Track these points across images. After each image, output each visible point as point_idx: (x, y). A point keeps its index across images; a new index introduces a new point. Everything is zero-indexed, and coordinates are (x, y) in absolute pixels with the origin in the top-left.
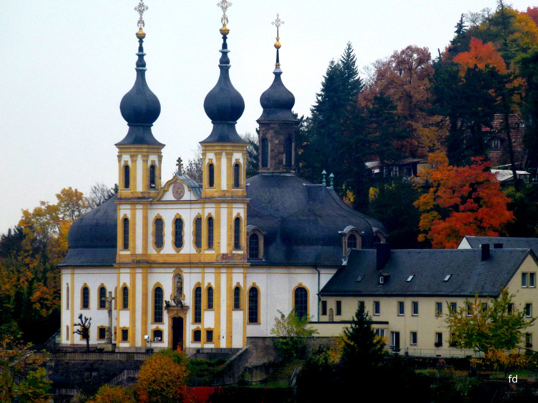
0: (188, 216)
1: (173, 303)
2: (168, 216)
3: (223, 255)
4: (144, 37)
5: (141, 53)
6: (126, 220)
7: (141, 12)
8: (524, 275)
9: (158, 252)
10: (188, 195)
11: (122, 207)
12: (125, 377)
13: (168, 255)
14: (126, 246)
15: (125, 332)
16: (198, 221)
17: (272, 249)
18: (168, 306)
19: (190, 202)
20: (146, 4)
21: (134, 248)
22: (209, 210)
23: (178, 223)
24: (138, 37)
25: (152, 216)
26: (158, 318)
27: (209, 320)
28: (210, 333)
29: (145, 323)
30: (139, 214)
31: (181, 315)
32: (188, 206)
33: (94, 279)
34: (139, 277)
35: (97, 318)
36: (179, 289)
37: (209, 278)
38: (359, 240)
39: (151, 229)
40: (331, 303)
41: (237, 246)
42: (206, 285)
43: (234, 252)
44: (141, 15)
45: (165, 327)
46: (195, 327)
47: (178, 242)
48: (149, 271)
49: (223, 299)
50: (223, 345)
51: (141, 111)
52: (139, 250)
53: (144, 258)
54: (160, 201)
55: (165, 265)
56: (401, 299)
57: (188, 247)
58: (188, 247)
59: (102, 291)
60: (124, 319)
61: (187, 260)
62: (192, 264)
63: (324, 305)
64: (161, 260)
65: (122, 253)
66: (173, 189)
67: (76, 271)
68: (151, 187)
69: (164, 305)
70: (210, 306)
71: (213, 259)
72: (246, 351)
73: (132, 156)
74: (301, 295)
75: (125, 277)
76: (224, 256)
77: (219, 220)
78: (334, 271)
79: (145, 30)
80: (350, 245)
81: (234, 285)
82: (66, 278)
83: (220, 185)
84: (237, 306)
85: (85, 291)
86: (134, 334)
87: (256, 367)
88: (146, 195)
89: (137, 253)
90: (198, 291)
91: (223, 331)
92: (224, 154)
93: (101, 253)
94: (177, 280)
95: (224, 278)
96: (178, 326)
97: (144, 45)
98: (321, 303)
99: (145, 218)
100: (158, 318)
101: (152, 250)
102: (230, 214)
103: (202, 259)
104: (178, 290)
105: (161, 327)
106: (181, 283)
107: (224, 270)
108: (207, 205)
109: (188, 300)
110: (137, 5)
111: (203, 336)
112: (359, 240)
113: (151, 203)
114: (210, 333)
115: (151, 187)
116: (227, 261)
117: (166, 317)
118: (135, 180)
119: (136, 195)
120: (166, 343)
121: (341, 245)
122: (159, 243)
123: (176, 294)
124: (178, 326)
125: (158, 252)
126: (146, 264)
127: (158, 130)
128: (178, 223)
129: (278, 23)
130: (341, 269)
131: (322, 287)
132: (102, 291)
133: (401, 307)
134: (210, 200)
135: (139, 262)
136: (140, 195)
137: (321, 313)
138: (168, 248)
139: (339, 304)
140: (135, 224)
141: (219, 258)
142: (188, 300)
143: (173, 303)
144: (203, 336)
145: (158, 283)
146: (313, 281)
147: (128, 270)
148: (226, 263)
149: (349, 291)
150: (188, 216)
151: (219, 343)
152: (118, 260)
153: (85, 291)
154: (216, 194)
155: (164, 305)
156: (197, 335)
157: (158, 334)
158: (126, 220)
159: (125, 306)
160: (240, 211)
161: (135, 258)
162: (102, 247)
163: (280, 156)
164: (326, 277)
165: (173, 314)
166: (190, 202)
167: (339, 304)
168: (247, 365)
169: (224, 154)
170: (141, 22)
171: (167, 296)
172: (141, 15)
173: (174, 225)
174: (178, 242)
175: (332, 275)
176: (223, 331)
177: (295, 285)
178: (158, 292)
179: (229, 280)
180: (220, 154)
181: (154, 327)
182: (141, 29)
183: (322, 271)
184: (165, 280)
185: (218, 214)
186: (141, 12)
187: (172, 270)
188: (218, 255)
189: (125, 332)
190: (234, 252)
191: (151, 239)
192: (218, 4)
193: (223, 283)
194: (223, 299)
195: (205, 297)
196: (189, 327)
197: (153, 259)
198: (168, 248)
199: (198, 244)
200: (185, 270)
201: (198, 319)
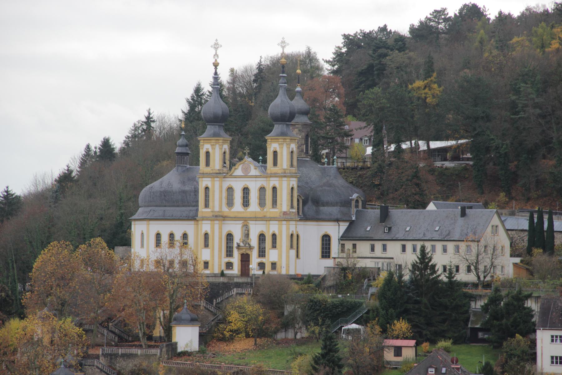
0: (254, 187)
2: (238, 186)
3: (284, 212)
4: (218, 66)
5: (216, 76)
6: (207, 188)
7: (216, 49)
8: (493, 226)
9: (230, 210)
10: (254, 172)
12: (234, 293)
13: (238, 212)
14: (207, 206)
15: (206, 264)
16: (262, 190)
17: (306, 208)
18: (238, 246)
19: (256, 177)
20: (220, 43)
21: (213, 207)
22: (274, 182)
23: (246, 191)
24: (214, 65)
26: (229, 253)
27: (272, 255)
28: (274, 265)
29: (220, 258)
31: (248, 252)
32: (254, 179)
34: (217, 227)
36: (247, 235)
37: (274, 227)
38: (360, 204)
39: (224, 194)
40: (349, 245)
41: (292, 207)
42: (271, 232)
43: (291, 210)
44: (216, 51)
45: (236, 260)
46: (260, 260)
47: (246, 203)
49: (283, 241)
50: (284, 272)
52: (217, 209)
53: (220, 214)
54: (232, 176)
56: (404, 243)
57: (254, 206)
58: (254, 206)
59: (172, 235)
62: (256, 219)
63: (343, 245)
64: (232, 215)
67: (151, 222)
68: (224, 166)
70: (274, 246)
71: (277, 215)
72: (325, 276)
73: (212, 145)
74: (326, 239)
76: (285, 213)
77: (281, 189)
78: (347, 224)
79: (218, 61)
80: (357, 206)
81: (291, 233)
83: (282, 165)
84: (292, 247)
85: (158, 236)
86: (213, 265)
87: (330, 287)
88: (221, 172)
89: (215, 210)
90: (262, 237)
91: (284, 264)
92: (285, 144)
93: (185, 211)
94: (244, 228)
95: (284, 227)
96: (245, 259)
97: (218, 70)
98: (340, 245)
99: (221, 187)
100: (229, 253)
101: (225, 209)
102: (289, 185)
103: (268, 215)
104: (245, 236)
106: (248, 231)
107: (284, 222)
110: (213, 44)
112: (360, 204)
113: (225, 177)
114: (274, 265)
115: (224, 166)
116: (287, 216)
118: (214, 161)
119: (214, 171)
120: (236, 270)
121: (351, 206)
122: (230, 203)
123: (244, 238)
124: (245, 259)
125: (230, 210)
126: (221, 218)
128: (246, 191)
130: (352, 223)
131: (341, 234)
132: (172, 235)
133: (404, 248)
134: (275, 175)
135: (216, 216)
136: (218, 172)
137: (340, 251)
139: (354, 246)
140: (214, 191)
141: (282, 214)
142: (254, 241)
143: (242, 244)
146: (335, 231)
148: (285, 217)
149: (353, 237)
150: (254, 187)
151: (281, 271)
152: (200, 215)
153: (158, 236)
154: (280, 172)
155: (235, 245)
156: (262, 266)
157: (229, 265)
158: (207, 188)
159: (206, 245)
161: (214, 214)
162: (169, 206)
164: (344, 226)
166: (256, 177)
167: (354, 246)
168: (325, 285)
169: (285, 144)
170: (216, 55)
171: (237, 239)
172: (216, 51)
173: (242, 192)
174: (246, 203)
175: (346, 227)
176: (284, 264)
177: (323, 233)
178: (230, 237)
179: (288, 229)
180: (282, 144)
182: (216, 60)
183: (341, 223)
185: (281, 185)
186: (216, 49)
188: (281, 212)
189: (206, 264)
190: (291, 210)
191: (224, 201)
192: (278, 44)
193: (283, 231)
194: (283, 241)
196: (255, 260)
197: (225, 214)
199: (262, 203)
200: (250, 222)
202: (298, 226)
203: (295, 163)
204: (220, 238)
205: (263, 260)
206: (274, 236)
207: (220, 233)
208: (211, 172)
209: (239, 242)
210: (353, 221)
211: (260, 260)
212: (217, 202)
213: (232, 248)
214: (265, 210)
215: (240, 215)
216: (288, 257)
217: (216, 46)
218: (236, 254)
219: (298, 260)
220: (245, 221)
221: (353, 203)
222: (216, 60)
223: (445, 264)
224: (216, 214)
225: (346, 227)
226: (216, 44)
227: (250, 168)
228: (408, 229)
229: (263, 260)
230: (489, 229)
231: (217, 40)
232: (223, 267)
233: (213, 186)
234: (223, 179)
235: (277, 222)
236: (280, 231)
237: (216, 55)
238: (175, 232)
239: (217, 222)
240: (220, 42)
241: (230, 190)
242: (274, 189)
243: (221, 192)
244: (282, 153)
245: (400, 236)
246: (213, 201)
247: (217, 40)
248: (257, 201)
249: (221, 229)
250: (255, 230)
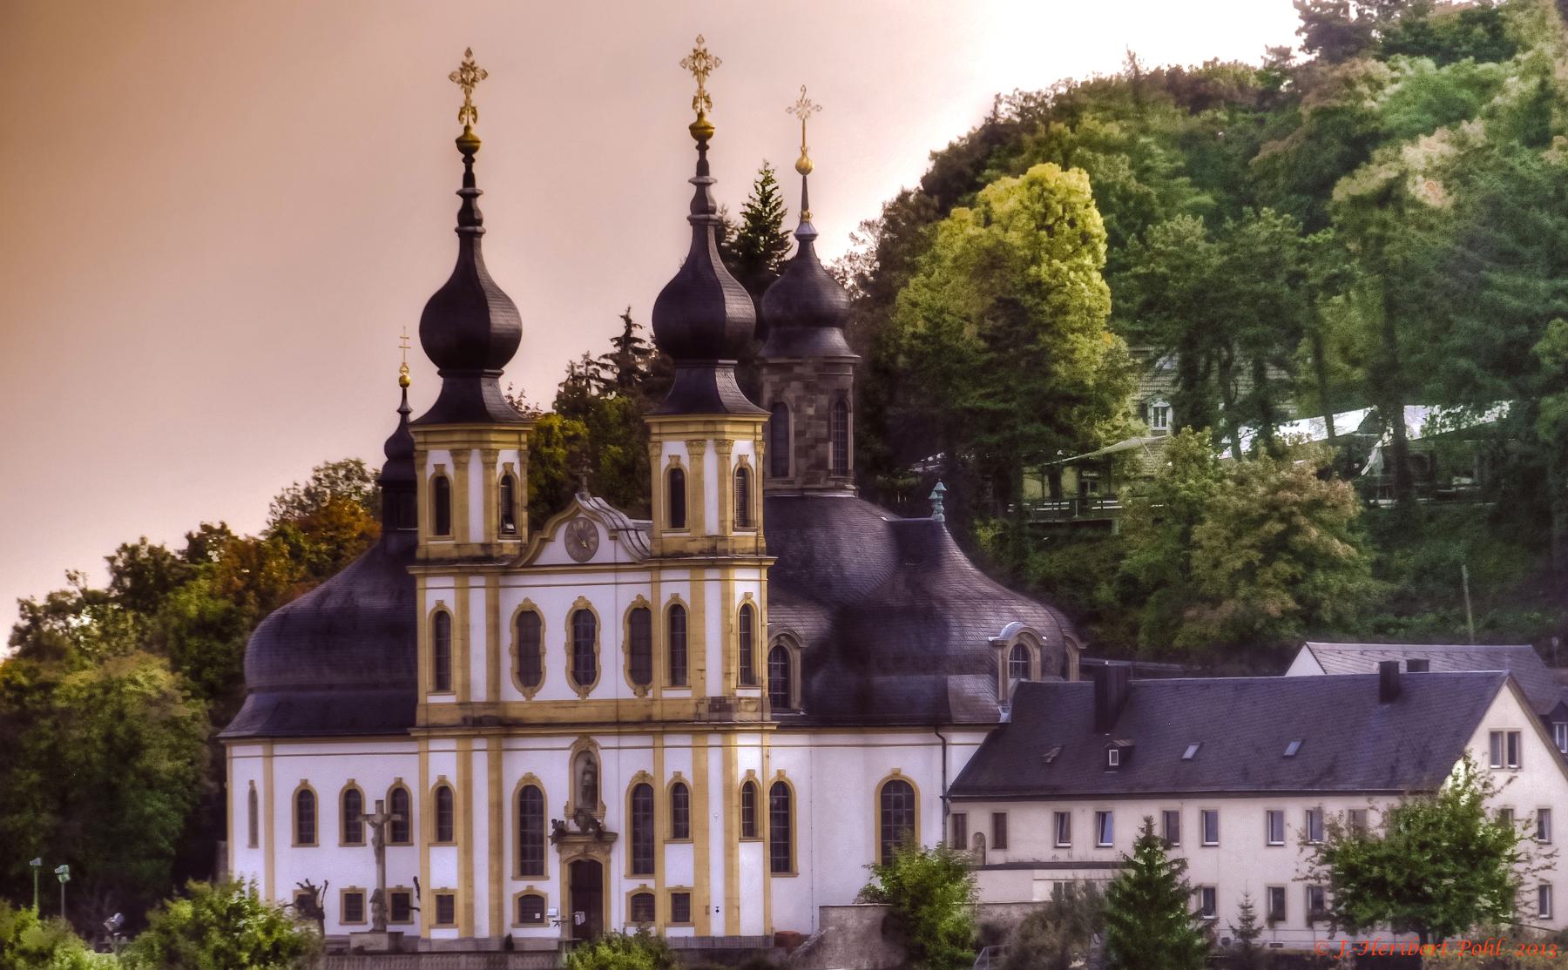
0: (610, 602)
1: (573, 827)
2: (554, 601)
3: (713, 699)
4: (475, 149)
5: (469, 190)
6: (441, 617)
8: (1494, 736)
9: (529, 698)
11: (431, 582)
13: (558, 704)
14: (442, 684)
16: (639, 617)
21: (466, 686)
22: (675, 586)
23: (583, 624)
25: (513, 601)
26: (531, 864)
27: (676, 865)
28: (682, 904)
29: (497, 879)
31: (596, 855)
32: (610, 578)
33: (329, 769)
34: (480, 762)
35: (341, 867)
36: (588, 788)
39: (508, 638)
40: (979, 820)
42: (668, 777)
43: (740, 693)
44: (468, 93)
45: (553, 886)
46: (634, 884)
47: (584, 669)
48: (506, 744)
49: (715, 813)
50: (717, 927)
52: (480, 693)
55: (549, 727)
57: (613, 683)
58: (613, 683)
59: (351, 799)
60: (444, 869)
61: (609, 715)
62: (620, 724)
64: (536, 716)
65: (433, 701)
66: (567, 536)
69: (550, 830)
70: (681, 831)
73: (455, 453)
75: (443, 761)
77: (701, 611)
78: (979, 738)
79: (476, 131)
83: (700, 522)
85: (305, 802)
86: (470, 908)
90: (641, 795)
92: (710, 442)
94: (581, 765)
96: (586, 886)
97: (476, 169)
98: (949, 819)
99: (494, 611)
100: (531, 864)
101: (512, 693)
103: (657, 712)
104: (584, 795)
105: (539, 886)
108: (666, 575)
109: (616, 816)
112: (1036, 657)
113: (507, 572)
114: (682, 904)
117: (554, 863)
119: (467, 552)
122: (530, 671)
123: (579, 803)
124: (586, 886)
125: (529, 698)
126: (495, 726)
128: (583, 624)
129: (468, 75)
132: (351, 799)
136: (480, 553)
138: (556, 684)
139: (999, 822)
140: (466, 627)
141: (703, 709)
142: (616, 816)
143: (573, 827)
145: (530, 777)
147: (451, 744)
151: (708, 924)
152: (421, 717)
153: (305, 802)
154: (693, 547)
156: (642, 905)
157: (531, 908)
158: (441, 617)
160: (748, 585)
161: (469, 713)
163: (820, 448)
164: (962, 749)
165: (573, 853)
166: (616, 567)
167: (999, 822)
169: (710, 442)
170: (468, 110)
172: (468, 93)
173: (570, 628)
174: (584, 669)
177: (883, 773)
178: (531, 798)
180: (701, 443)
181: (522, 886)
183: (956, 738)
184: (549, 767)
187: (567, 742)
188: (700, 702)
189: (445, 907)
190: (740, 693)
191: (508, 663)
195: (663, 813)
196: (620, 885)
197: (514, 713)
198: (556, 684)
199: (639, 672)
201: (643, 862)
202: (774, 752)
203: (758, 514)
204: (497, 807)
205: (650, 884)
206: (679, 791)
207: (497, 784)
208: (455, 554)
209: (560, 817)
210: (1004, 725)
211: (634, 884)
212: (479, 669)
213: (541, 841)
214: (650, 695)
215: (564, 715)
218: (554, 863)
219: (781, 884)
220: (584, 732)
222: (467, 128)
223: (1277, 881)
224: (477, 714)
225: (970, 752)
226: (467, 67)
227: (596, 534)
228: (1292, 748)
229: (650, 884)
231: (469, 53)
232: (510, 912)
233: (464, 606)
234: (502, 581)
235: (686, 740)
236: (701, 774)
237: (468, 110)
238: (316, 785)
239: (480, 744)
240: (480, 61)
241: (529, 622)
242: (677, 613)
243: (494, 629)
244: (699, 475)
246: (466, 667)
247: (469, 53)
248: (622, 659)
249: (496, 767)
250: (621, 765)
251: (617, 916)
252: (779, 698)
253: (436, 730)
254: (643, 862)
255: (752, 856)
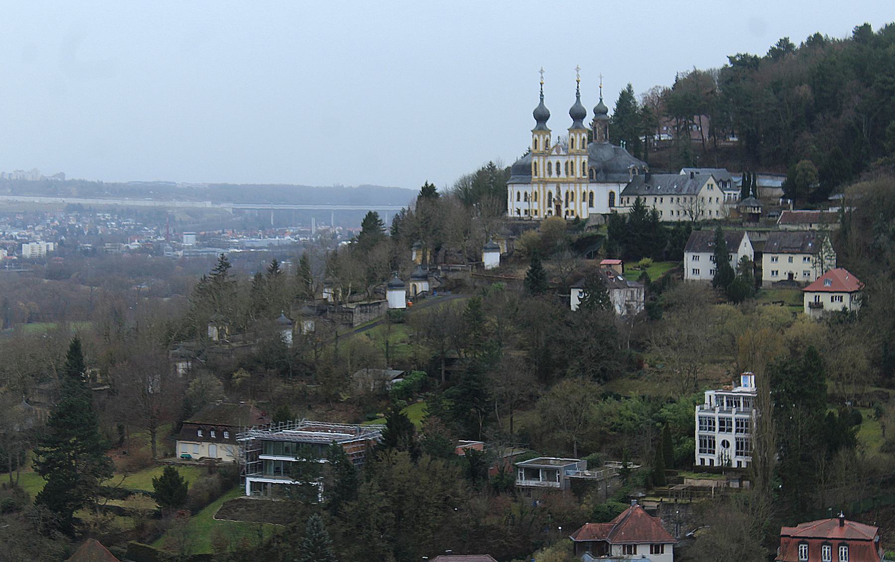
10: (562, 153)
15: (536, 211)
16: (567, 163)
22: (572, 158)
23: (558, 164)
26: (550, 206)
27: (571, 206)
28: (572, 212)
30: (541, 160)
33: (522, 189)
34: (541, 188)
35: (523, 206)
36: (559, 193)
37: (572, 188)
39: (546, 167)
41: (584, 175)
45: (553, 209)
47: (558, 173)
49: (578, 197)
51: (541, 117)
52: (542, 176)
55: (553, 182)
57: (563, 175)
58: (563, 175)
59: (526, 194)
60: (535, 206)
62: (564, 182)
74: (612, 195)
75: (535, 188)
82: (510, 188)
96: (558, 208)
101: (547, 176)
109: (563, 198)
111: (570, 213)
114: (572, 212)
122: (550, 173)
124: (558, 208)
126: (545, 182)
127: (548, 124)
128: (558, 164)
130: (629, 184)
132: (526, 194)
134: (572, 154)
142: (563, 198)
144: (570, 213)
146: (618, 189)
148: (579, 181)
153: (519, 193)
156: (567, 212)
157: (550, 212)
160: (585, 159)
164: (623, 187)
171: (554, 196)
174: (558, 173)
178: (550, 194)
179: (580, 189)
184: (553, 189)
189: (536, 211)
191: (547, 172)
194: (578, 197)
195: (570, 196)
196: (563, 210)
198: (554, 175)
199: (567, 173)
201: (567, 206)
207: (544, 192)
212: (542, 173)
216: (581, 207)
217: (542, 72)
220: (558, 184)
221: (631, 171)
230: (706, 185)
241: (550, 164)
245: (654, 192)
251: (563, 214)
252: (591, 177)
253: (535, 183)
254: (567, 206)
255: (585, 204)
